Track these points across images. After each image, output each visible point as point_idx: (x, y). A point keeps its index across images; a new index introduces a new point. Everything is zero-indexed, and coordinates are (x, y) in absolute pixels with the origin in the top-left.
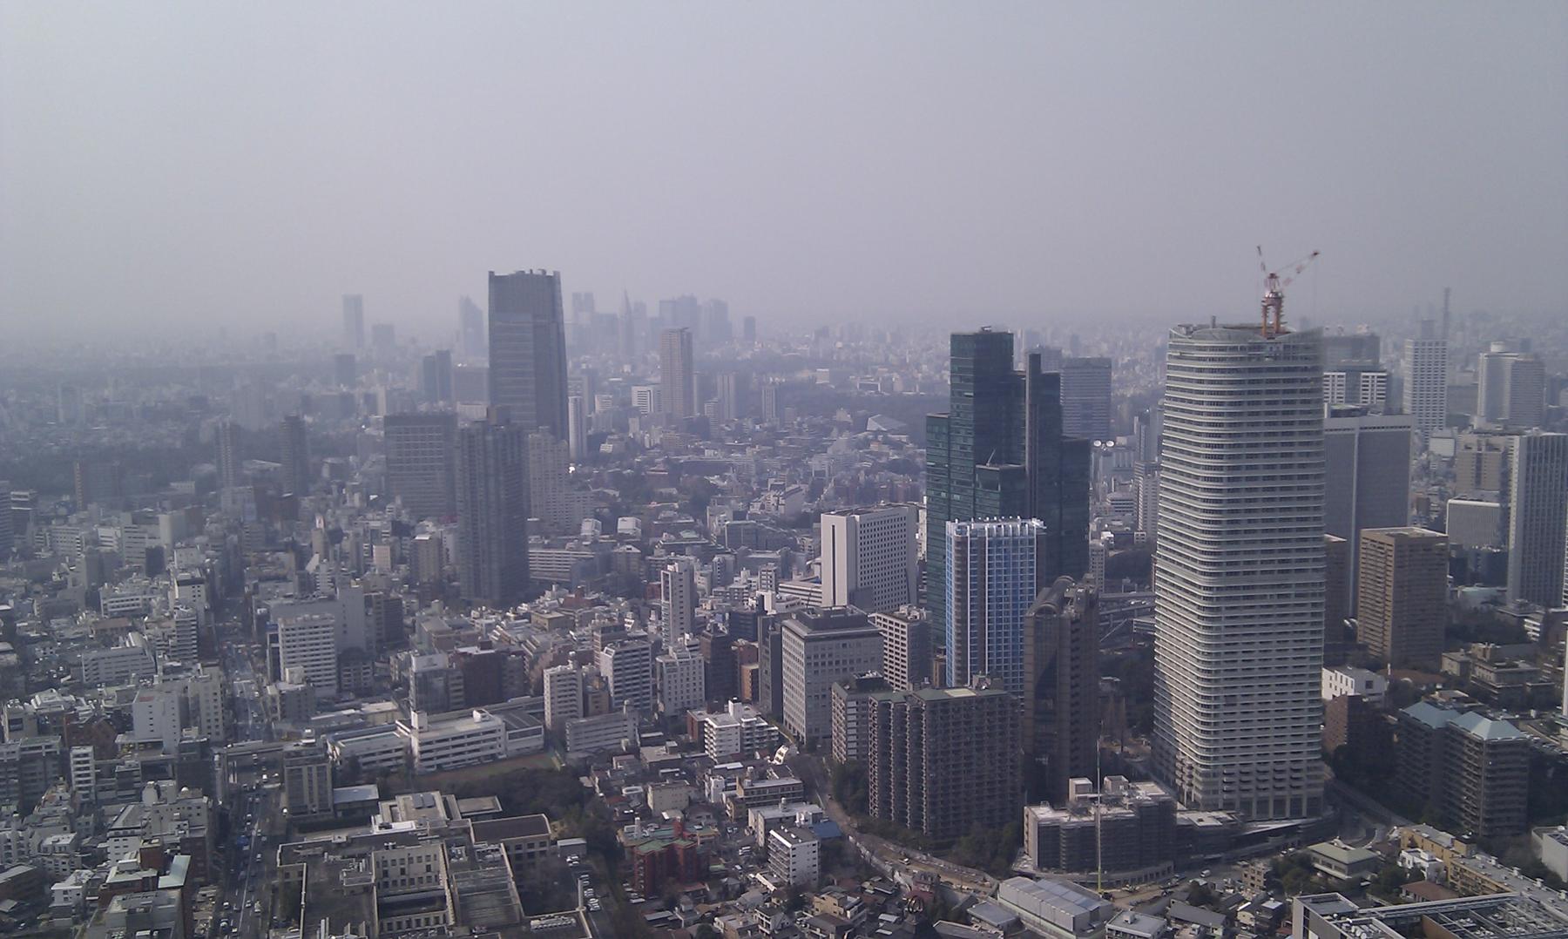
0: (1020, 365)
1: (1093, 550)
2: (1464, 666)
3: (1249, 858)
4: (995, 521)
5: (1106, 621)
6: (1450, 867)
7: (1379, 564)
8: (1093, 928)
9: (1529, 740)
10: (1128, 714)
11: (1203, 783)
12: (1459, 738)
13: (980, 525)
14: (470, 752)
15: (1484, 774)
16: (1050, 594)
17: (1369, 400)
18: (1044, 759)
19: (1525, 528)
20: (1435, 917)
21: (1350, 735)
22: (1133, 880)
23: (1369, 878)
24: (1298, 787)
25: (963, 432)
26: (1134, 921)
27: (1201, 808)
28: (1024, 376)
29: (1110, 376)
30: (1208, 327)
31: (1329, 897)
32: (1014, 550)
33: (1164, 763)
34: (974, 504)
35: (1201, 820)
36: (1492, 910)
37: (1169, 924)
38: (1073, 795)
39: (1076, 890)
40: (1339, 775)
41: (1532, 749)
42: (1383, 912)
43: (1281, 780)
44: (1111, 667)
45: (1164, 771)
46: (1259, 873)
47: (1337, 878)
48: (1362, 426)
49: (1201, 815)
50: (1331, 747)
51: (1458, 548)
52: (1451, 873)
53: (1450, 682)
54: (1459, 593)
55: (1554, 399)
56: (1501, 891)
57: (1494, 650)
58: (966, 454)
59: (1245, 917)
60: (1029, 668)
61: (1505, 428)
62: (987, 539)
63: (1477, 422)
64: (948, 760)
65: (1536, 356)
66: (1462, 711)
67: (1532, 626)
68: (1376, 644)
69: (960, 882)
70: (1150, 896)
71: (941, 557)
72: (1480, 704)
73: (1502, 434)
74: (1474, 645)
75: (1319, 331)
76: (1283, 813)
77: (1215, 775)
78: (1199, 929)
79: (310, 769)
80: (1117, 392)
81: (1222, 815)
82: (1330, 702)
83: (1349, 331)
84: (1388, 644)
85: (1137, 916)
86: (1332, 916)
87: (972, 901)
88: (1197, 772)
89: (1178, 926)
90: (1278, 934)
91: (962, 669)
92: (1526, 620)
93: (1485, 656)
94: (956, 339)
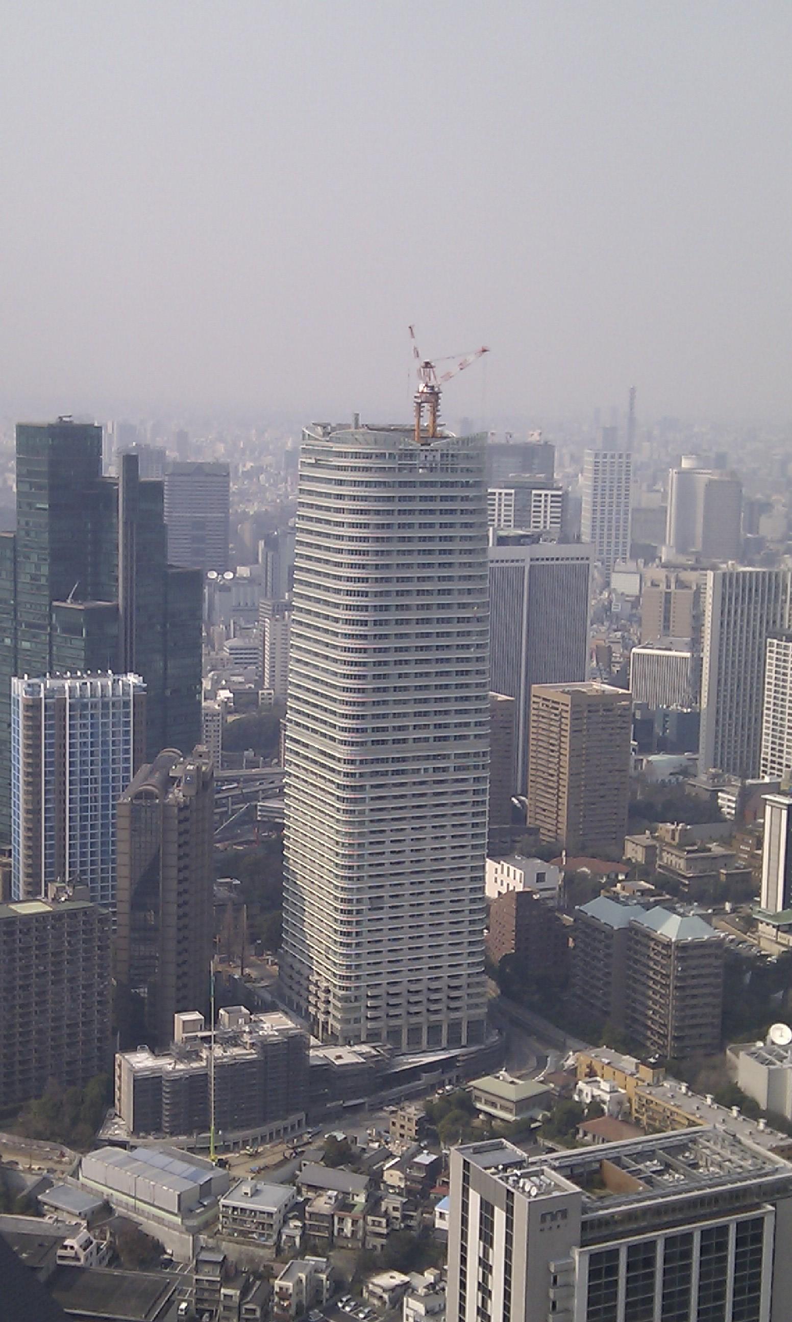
1: (207, 715)
2: (650, 850)
3: (397, 1101)
4: (79, 678)
5: (224, 805)
6: (635, 1099)
7: (552, 728)
8: (204, 1206)
9: (724, 938)
10: (251, 926)
11: (344, 1010)
12: (644, 940)
13: (57, 683)
15: (672, 982)
16: (152, 772)
17: (541, 525)
18: (142, 990)
19: (719, 682)
20: (617, 1161)
21: (518, 939)
22: (255, 1140)
23: (540, 1118)
24: (457, 1009)
25: (34, 558)
26: (256, 1192)
27: (341, 1041)
28: (117, 484)
29: (228, 486)
30: (349, 426)
31: (492, 1145)
32: (105, 716)
33: (296, 987)
34: (50, 653)
35: (339, 1057)
36: (682, 1148)
37: (299, 1192)
38: (179, 1034)
39: (183, 1159)
40: (506, 991)
41: (727, 950)
42: (557, 1159)
43: (437, 1001)
44: (228, 868)
45: (295, 998)
46: (409, 1120)
47: (502, 1120)
48: (533, 557)
49: (339, 1051)
50: (497, 956)
51: (644, 707)
52: (635, 1106)
53: (634, 871)
54: (645, 761)
55: (752, 526)
56: (692, 1124)
57: (684, 831)
58: (39, 588)
59: (393, 1177)
60: (124, 871)
61: (697, 560)
62: (68, 701)
63: (665, 553)
64: (14, 997)
65: (733, 473)
66: (648, 907)
67: (727, 802)
68: (549, 826)
69: (28, 1160)
70: (279, 1158)
71: (5, 726)
72: (668, 897)
73: (693, 569)
74: (661, 825)
75: (483, 436)
76: (439, 1042)
77: (357, 999)
78: (336, 1197)
80: (238, 507)
81: (365, 1048)
82: (495, 901)
83: (518, 438)
84: (563, 826)
85: (259, 1187)
86: (496, 1168)
87: (45, 1184)
88: (335, 996)
89: (311, 1195)
90: (432, 1196)
91: (33, 877)
92: (720, 794)
93: (673, 839)
94: (24, 431)
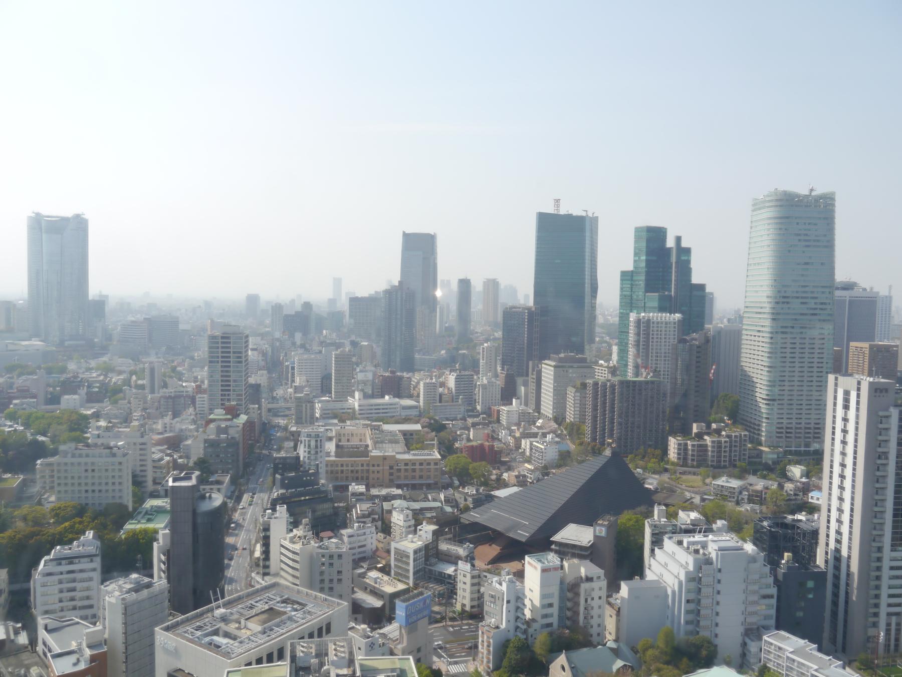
0: (670, 243)
14: (383, 413)
79: (306, 405)
